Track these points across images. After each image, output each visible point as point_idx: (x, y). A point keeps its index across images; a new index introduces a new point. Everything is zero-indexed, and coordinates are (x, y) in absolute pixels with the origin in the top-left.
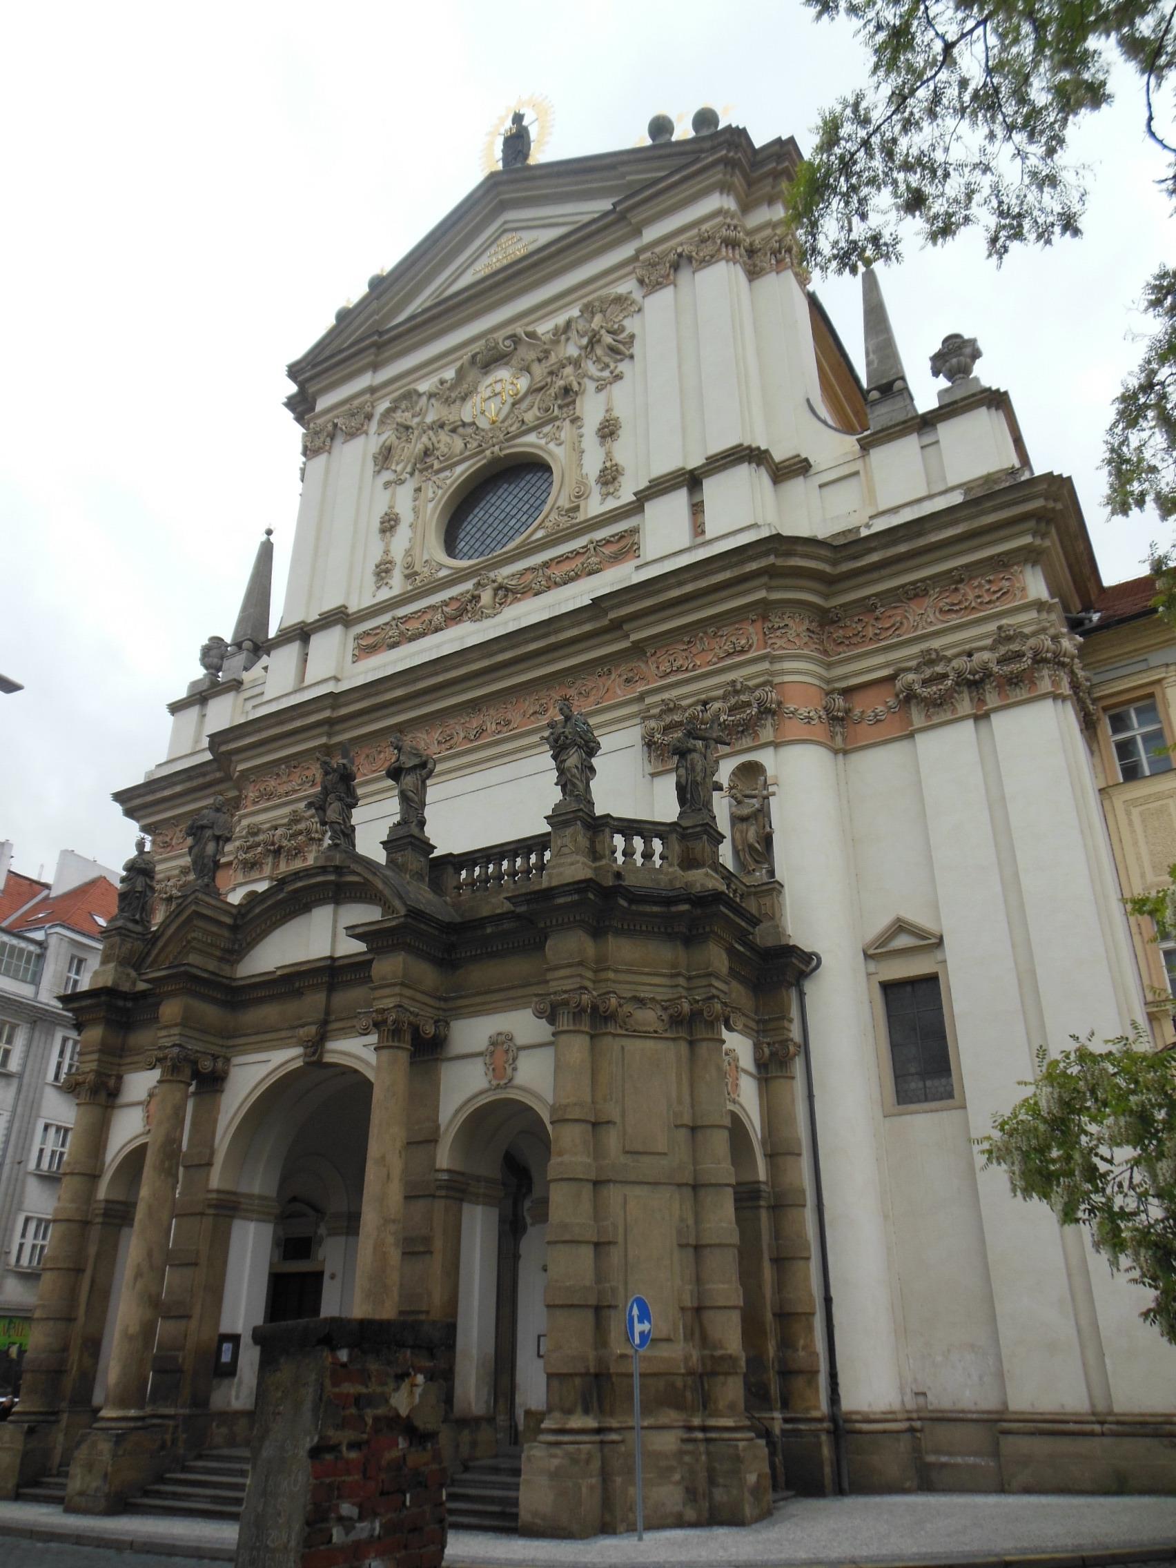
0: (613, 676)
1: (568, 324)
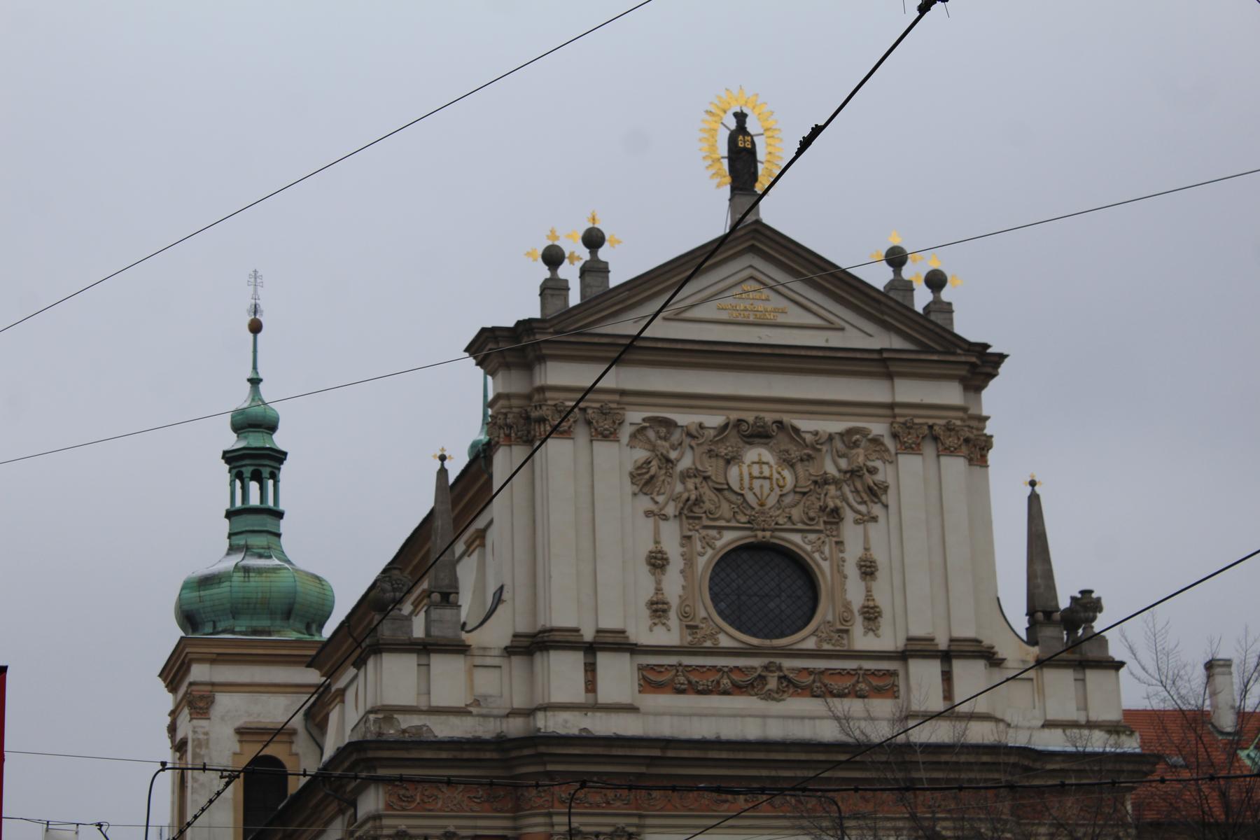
1: (831, 438)
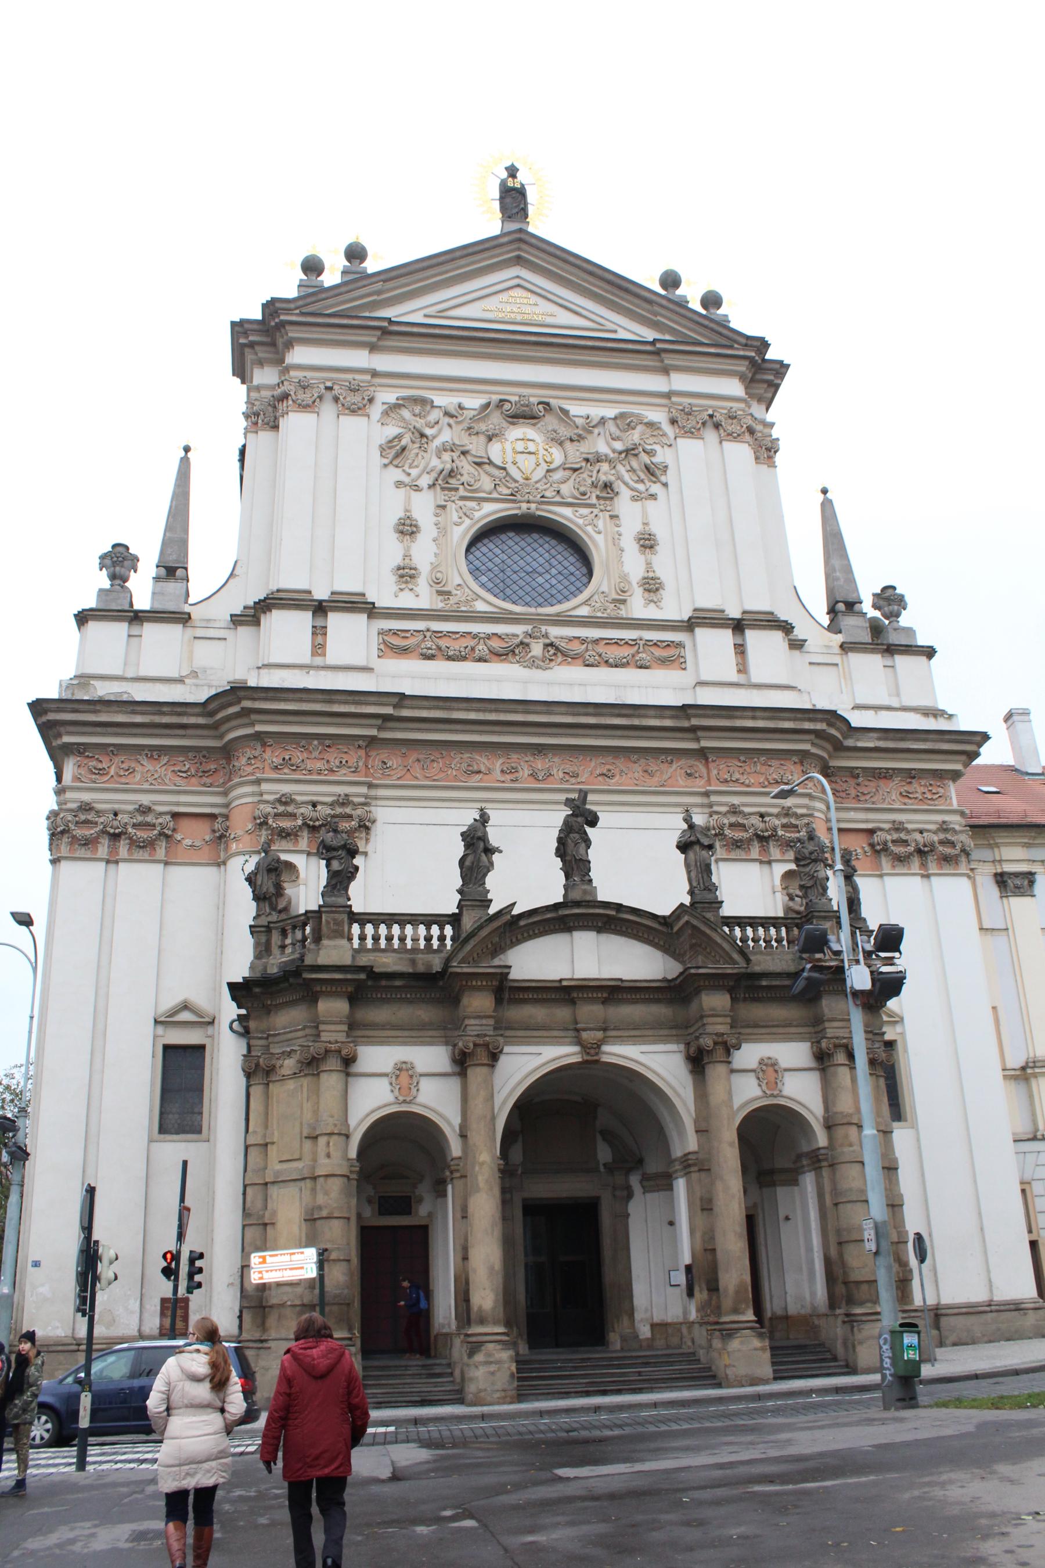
0: (674, 766)
1: (603, 421)
